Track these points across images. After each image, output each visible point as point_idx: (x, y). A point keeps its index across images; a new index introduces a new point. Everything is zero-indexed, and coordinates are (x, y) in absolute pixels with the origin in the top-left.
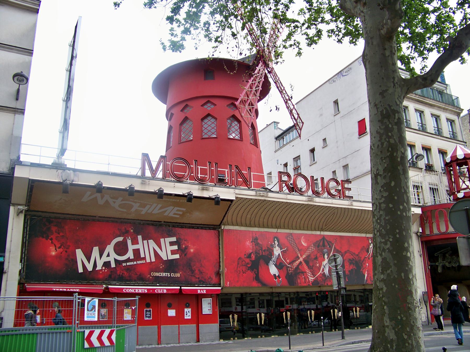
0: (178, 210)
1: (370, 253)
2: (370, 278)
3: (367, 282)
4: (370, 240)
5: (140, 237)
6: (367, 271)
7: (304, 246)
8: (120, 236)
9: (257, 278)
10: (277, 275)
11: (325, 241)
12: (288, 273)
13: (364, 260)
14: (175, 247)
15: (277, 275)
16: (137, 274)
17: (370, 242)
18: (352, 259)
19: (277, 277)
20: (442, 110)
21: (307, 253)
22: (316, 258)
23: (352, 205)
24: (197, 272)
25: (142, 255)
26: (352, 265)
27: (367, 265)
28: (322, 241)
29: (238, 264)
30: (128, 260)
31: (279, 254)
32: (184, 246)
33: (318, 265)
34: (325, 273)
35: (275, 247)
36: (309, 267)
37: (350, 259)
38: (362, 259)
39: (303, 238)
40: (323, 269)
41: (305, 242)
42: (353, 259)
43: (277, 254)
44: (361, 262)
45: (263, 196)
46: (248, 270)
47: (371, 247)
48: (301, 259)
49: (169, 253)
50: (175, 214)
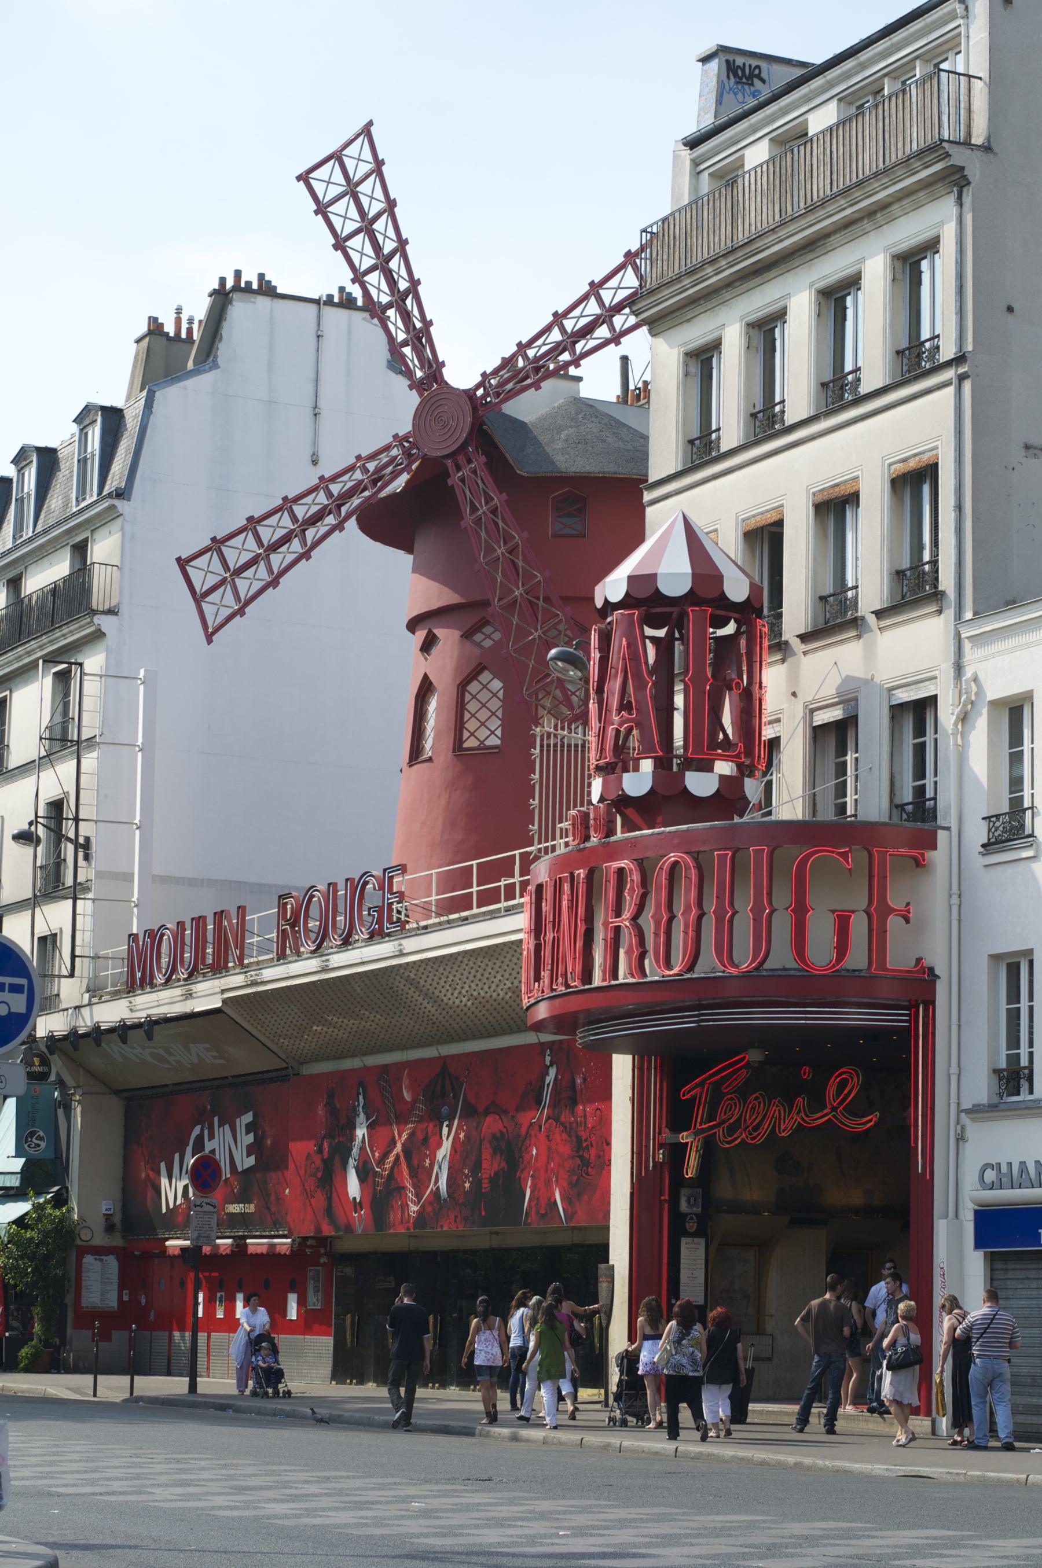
0: (205, 1049)
2: (537, 1203)
4: (548, 1052)
6: (532, 1176)
9: (329, 1211)
10: (358, 1200)
14: (250, 1138)
15: (358, 1200)
17: (548, 1059)
18: (498, 1135)
19: (358, 1207)
20: (867, 225)
22: (425, 1141)
23: (402, 954)
31: (364, 1135)
33: (428, 1161)
35: (358, 1115)
36: (414, 1174)
37: (494, 1137)
40: (437, 1174)
43: (361, 1137)
45: (255, 983)
47: (547, 1082)
48: (399, 1148)
50: (215, 1057)
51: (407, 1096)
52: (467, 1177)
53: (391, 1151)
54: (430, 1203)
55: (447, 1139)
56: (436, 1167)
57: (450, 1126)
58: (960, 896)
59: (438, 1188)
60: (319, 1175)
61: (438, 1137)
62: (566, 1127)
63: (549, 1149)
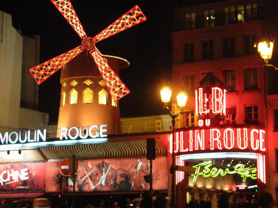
1: (138, 169)
3: (133, 189)
5: (12, 170)
7: (90, 168)
8: (5, 170)
11: (104, 164)
12: (78, 185)
13: (132, 174)
14: (27, 174)
16: (10, 188)
21: (91, 172)
22: (97, 175)
24: (36, 185)
25: (13, 179)
26: (122, 178)
27: (135, 177)
28: (102, 164)
29: (52, 180)
30: (8, 182)
32: (30, 173)
33: (98, 179)
34: (103, 184)
36: (93, 181)
37: (121, 174)
38: (131, 173)
39: (90, 163)
41: (91, 165)
42: (124, 174)
44: (130, 175)
46: (57, 183)
47: (139, 164)
48: (87, 176)
49: (24, 176)
51: (90, 166)
52: (112, 181)
53: (85, 176)
54: (99, 186)
55: (105, 174)
56: (101, 180)
57: (105, 172)
58: (267, 138)
59: (102, 184)
60: (58, 181)
61: (101, 174)
62: (145, 173)
63: (140, 177)
